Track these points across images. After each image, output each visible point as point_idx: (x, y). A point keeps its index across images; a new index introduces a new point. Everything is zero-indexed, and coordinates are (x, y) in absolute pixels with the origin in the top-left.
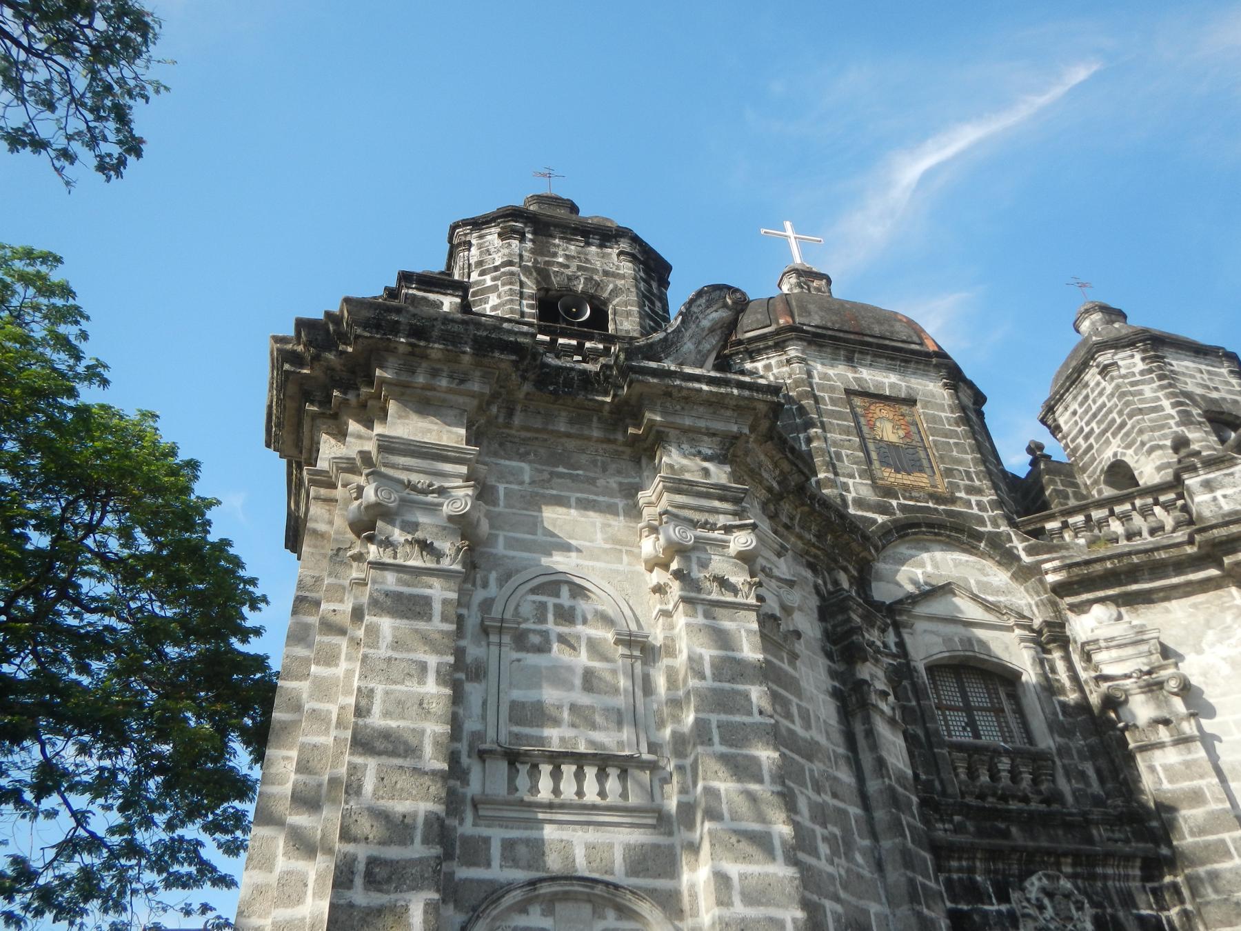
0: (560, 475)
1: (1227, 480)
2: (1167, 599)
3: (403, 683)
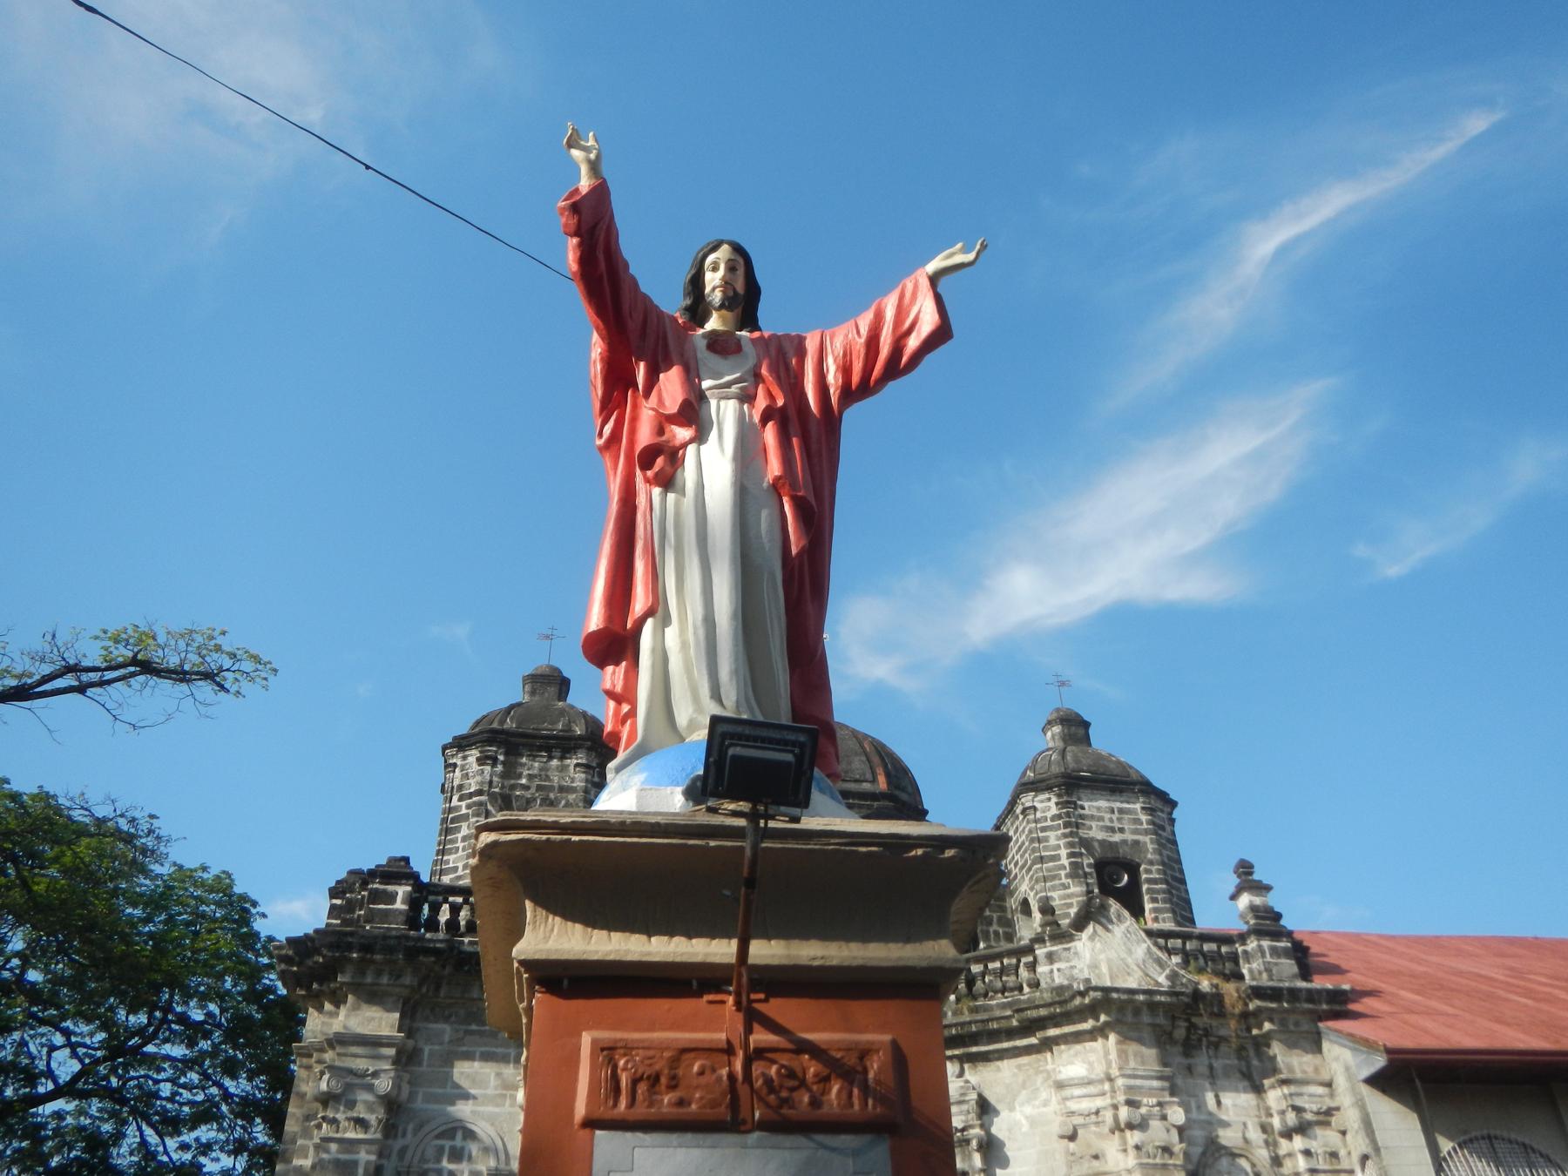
0: (472, 1033)
1: (1065, 954)
2: (1001, 1058)
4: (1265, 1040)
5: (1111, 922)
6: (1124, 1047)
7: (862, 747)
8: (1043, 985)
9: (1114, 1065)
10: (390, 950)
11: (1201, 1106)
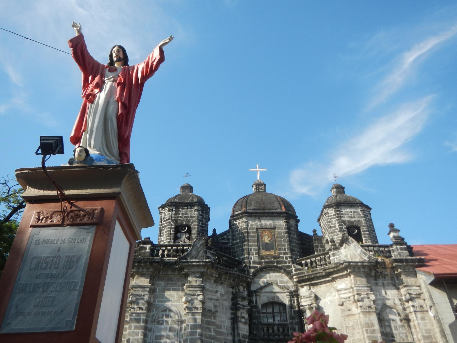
0: (170, 284)
1: (338, 253)
2: (321, 284)
3: (135, 336)
4: (399, 274)
5: (350, 243)
6: (356, 278)
7: (277, 199)
8: (332, 262)
9: (353, 284)
10: (145, 262)
11: (381, 294)
